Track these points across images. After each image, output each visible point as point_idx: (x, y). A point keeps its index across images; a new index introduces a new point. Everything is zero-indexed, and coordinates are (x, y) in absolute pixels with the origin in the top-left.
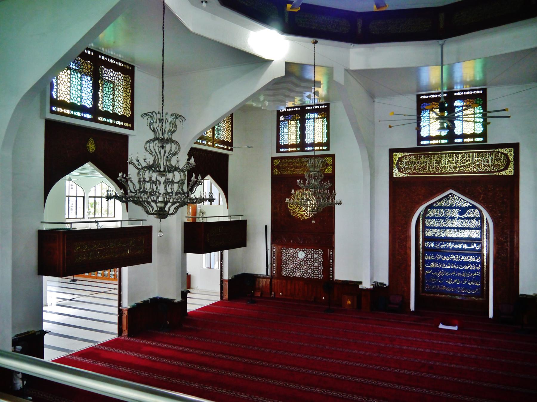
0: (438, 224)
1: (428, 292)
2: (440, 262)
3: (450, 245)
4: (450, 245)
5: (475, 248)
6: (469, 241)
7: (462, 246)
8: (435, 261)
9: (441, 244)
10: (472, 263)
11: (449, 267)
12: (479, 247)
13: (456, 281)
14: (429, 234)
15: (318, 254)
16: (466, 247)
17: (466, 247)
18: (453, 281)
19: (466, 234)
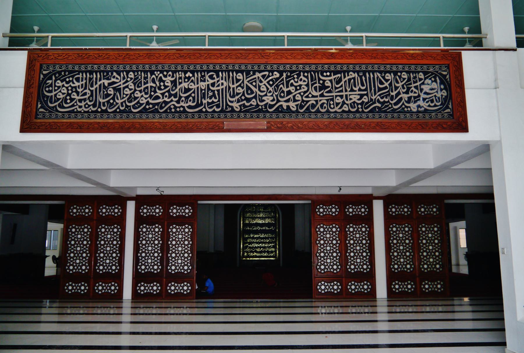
0: (252, 215)
1: (246, 257)
2: (253, 238)
3: (259, 228)
4: (259, 228)
5: (272, 229)
6: (268, 225)
7: (265, 228)
8: (250, 238)
9: (254, 227)
10: (271, 238)
11: (258, 241)
12: (274, 228)
13: (262, 249)
14: (247, 222)
15: (183, 233)
16: (267, 228)
17: (267, 228)
18: (260, 249)
19: (267, 221)
